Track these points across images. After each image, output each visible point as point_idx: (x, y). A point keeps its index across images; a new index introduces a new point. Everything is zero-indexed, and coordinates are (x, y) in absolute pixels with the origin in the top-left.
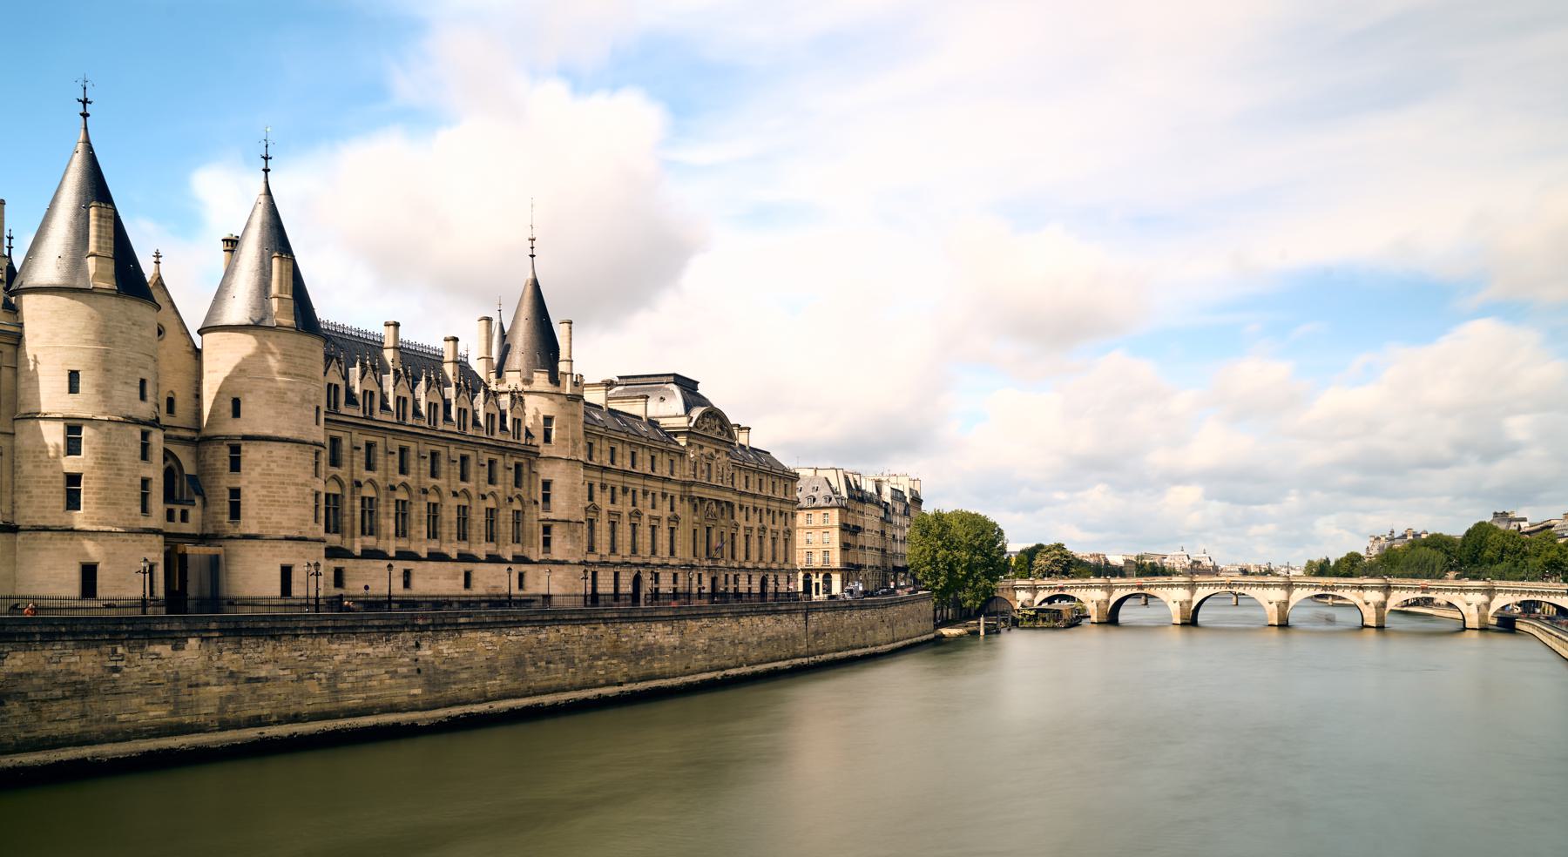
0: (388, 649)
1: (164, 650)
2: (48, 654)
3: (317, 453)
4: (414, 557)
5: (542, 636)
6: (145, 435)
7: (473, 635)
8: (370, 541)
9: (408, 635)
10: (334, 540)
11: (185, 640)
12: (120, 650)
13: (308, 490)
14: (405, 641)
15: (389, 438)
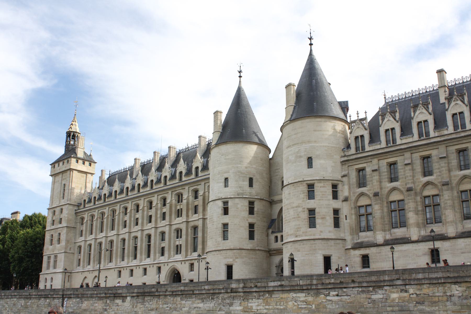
0: (212, 305)
1: (119, 301)
2: (91, 302)
3: (311, 187)
4: (443, 238)
5: (378, 296)
6: (226, 203)
7: (285, 295)
8: (399, 232)
9: (226, 296)
10: (365, 237)
11: (127, 296)
12: (108, 302)
13: (300, 209)
14: (224, 299)
15: (408, 155)
